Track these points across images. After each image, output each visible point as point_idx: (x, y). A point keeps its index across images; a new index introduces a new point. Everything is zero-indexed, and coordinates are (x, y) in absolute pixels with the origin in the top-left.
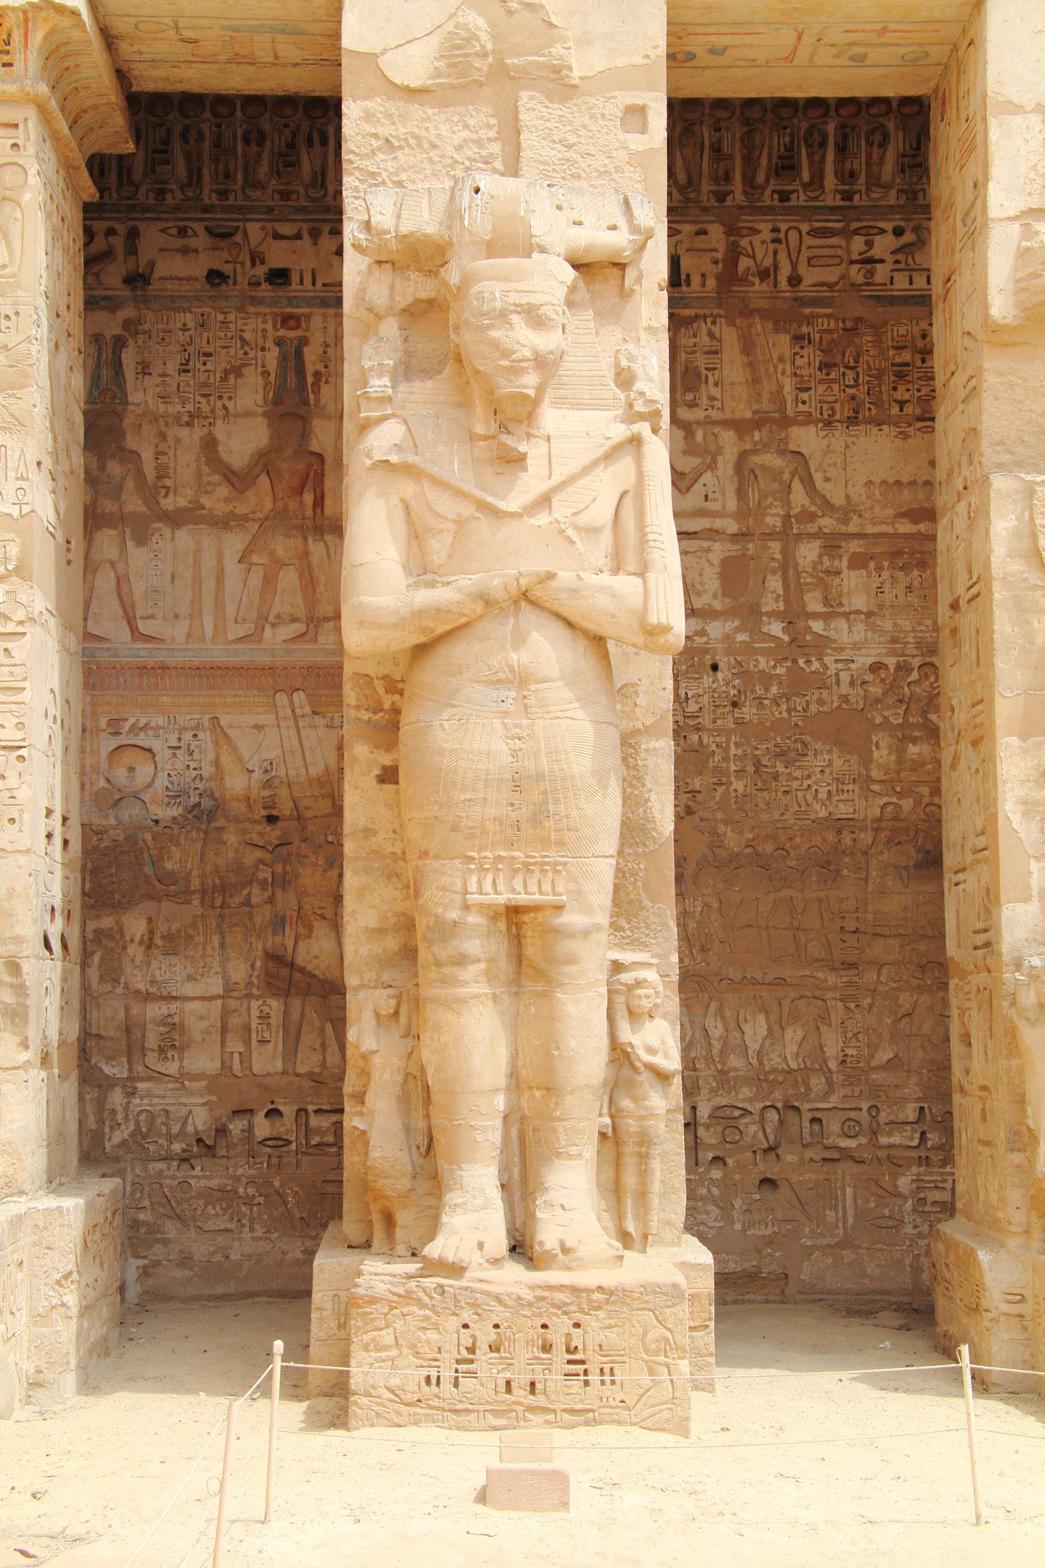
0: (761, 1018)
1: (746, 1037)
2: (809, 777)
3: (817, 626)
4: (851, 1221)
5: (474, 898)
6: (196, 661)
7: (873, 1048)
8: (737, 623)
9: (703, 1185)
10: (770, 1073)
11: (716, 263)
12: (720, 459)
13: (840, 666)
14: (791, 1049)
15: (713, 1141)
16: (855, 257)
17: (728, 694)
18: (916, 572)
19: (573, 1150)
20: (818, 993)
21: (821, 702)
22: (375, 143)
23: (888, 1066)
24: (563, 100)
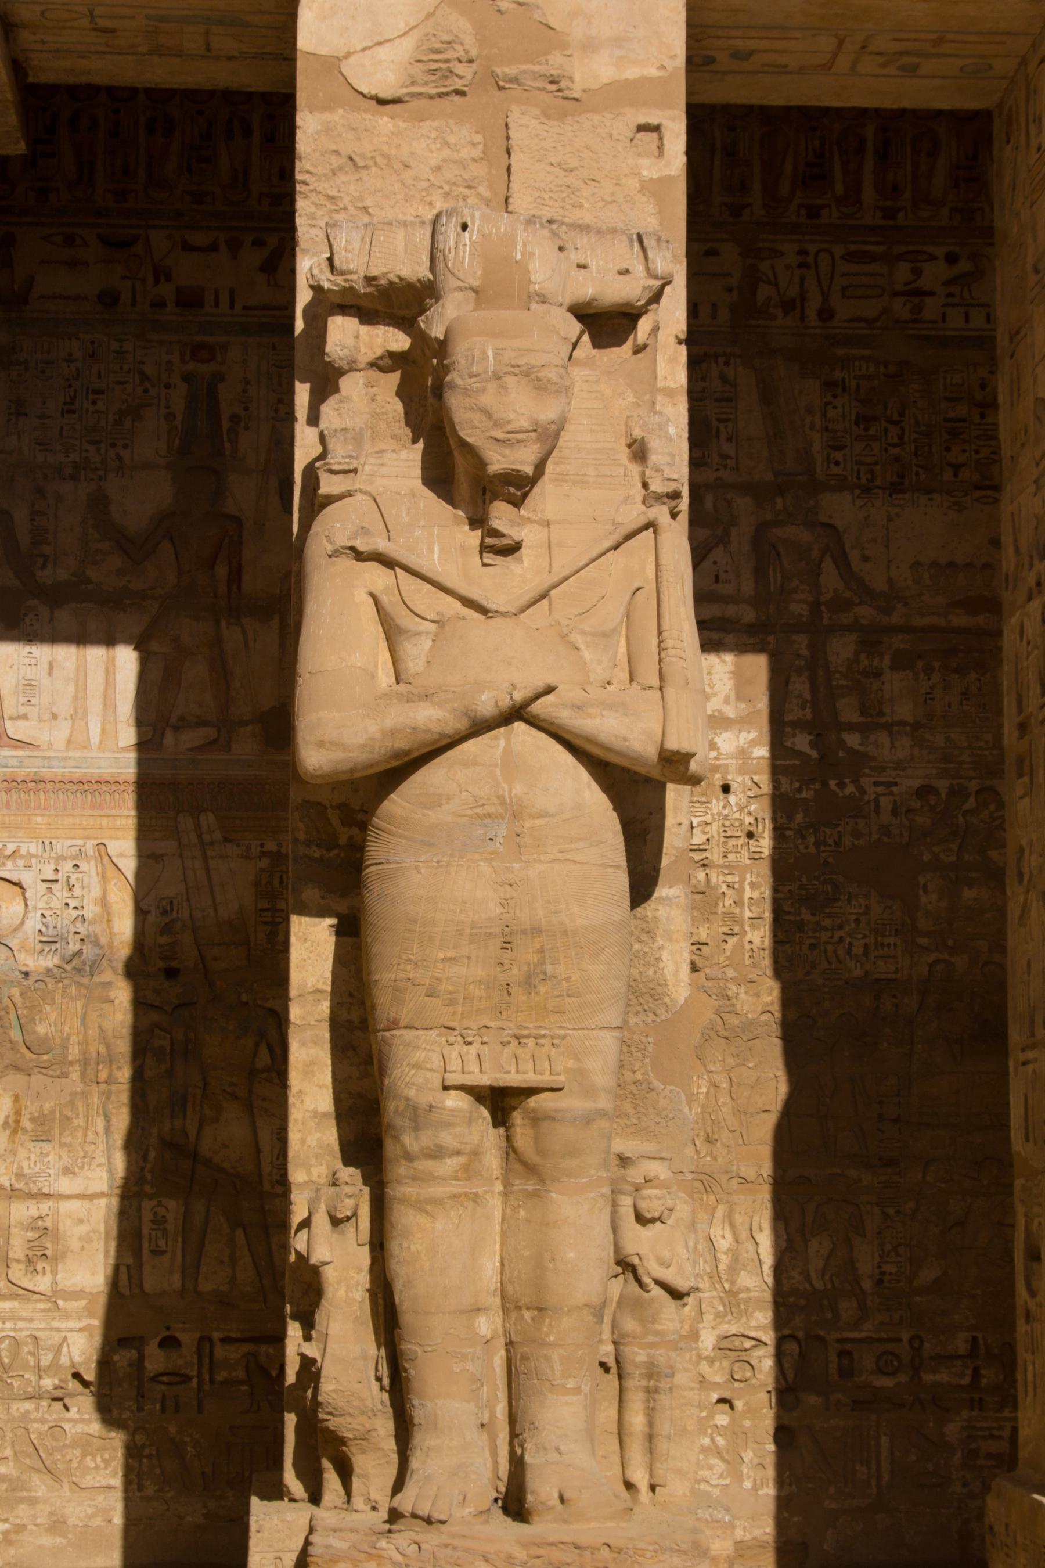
2: (841, 927)
3: (852, 740)
4: (886, 1477)
5: (455, 1078)
6: (79, 773)
8: (753, 735)
9: (705, 1434)
11: (730, 290)
12: (734, 531)
13: (880, 789)
14: (816, 1264)
15: (718, 1379)
16: (899, 287)
17: (742, 822)
18: (973, 675)
19: (571, 1384)
22: (336, 161)
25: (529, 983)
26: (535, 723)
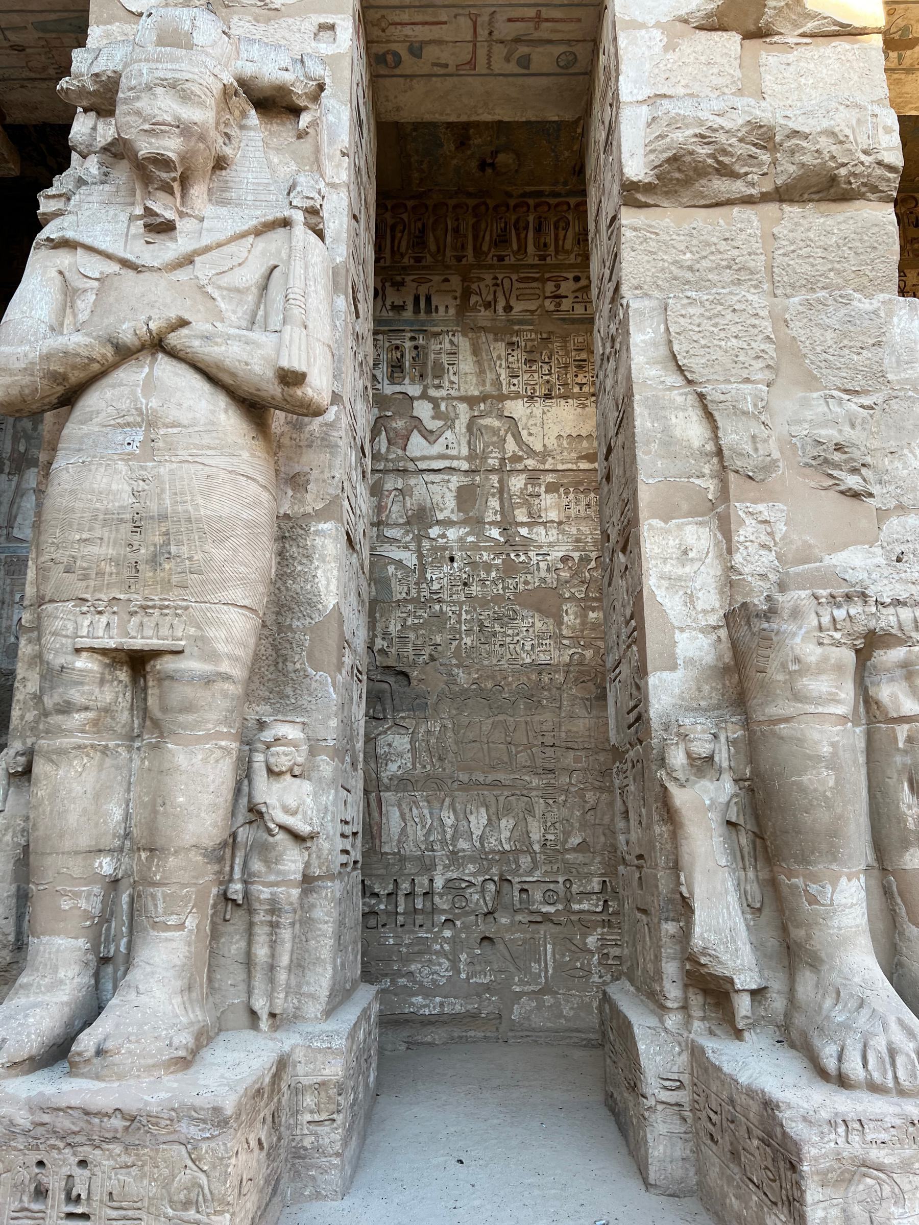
0: (483, 810)
1: (472, 825)
2: (518, 634)
3: (524, 531)
4: (550, 971)
7: (567, 834)
8: (467, 530)
9: (437, 943)
10: (489, 853)
11: (456, 298)
12: (457, 421)
13: (540, 558)
14: (505, 834)
15: (445, 907)
16: (548, 294)
17: (461, 577)
18: (592, 495)
19: (172, 920)
20: (525, 792)
21: (526, 583)
23: (579, 848)
24: (268, 20)
25: (154, 561)
26: (173, 354)
